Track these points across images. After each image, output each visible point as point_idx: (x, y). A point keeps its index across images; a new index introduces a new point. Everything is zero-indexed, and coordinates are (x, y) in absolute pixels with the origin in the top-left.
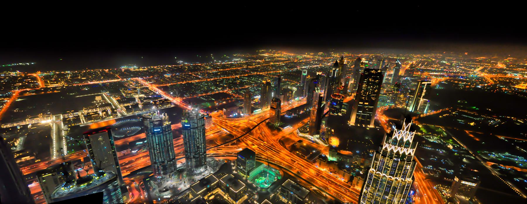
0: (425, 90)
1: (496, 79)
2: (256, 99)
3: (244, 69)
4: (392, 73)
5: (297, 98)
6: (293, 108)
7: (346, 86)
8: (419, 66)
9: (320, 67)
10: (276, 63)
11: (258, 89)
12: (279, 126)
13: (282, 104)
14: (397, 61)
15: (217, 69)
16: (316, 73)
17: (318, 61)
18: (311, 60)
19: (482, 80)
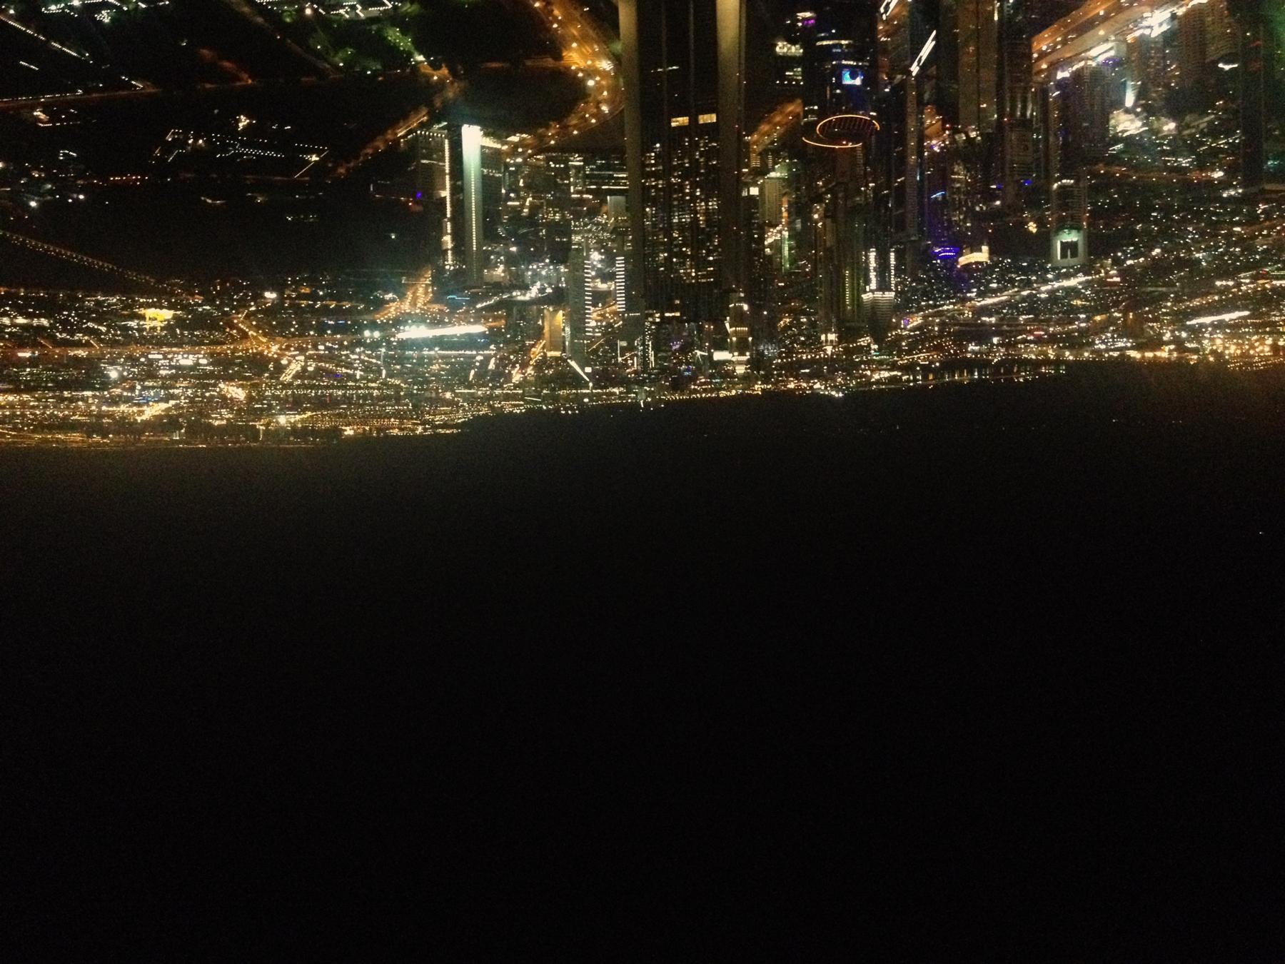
0: (447, 250)
1: (232, 335)
5: (1105, 64)
7: (800, 210)
8: (493, 361)
9: (971, 299)
14: (587, 374)
17: (981, 335)
19: (273, 322)
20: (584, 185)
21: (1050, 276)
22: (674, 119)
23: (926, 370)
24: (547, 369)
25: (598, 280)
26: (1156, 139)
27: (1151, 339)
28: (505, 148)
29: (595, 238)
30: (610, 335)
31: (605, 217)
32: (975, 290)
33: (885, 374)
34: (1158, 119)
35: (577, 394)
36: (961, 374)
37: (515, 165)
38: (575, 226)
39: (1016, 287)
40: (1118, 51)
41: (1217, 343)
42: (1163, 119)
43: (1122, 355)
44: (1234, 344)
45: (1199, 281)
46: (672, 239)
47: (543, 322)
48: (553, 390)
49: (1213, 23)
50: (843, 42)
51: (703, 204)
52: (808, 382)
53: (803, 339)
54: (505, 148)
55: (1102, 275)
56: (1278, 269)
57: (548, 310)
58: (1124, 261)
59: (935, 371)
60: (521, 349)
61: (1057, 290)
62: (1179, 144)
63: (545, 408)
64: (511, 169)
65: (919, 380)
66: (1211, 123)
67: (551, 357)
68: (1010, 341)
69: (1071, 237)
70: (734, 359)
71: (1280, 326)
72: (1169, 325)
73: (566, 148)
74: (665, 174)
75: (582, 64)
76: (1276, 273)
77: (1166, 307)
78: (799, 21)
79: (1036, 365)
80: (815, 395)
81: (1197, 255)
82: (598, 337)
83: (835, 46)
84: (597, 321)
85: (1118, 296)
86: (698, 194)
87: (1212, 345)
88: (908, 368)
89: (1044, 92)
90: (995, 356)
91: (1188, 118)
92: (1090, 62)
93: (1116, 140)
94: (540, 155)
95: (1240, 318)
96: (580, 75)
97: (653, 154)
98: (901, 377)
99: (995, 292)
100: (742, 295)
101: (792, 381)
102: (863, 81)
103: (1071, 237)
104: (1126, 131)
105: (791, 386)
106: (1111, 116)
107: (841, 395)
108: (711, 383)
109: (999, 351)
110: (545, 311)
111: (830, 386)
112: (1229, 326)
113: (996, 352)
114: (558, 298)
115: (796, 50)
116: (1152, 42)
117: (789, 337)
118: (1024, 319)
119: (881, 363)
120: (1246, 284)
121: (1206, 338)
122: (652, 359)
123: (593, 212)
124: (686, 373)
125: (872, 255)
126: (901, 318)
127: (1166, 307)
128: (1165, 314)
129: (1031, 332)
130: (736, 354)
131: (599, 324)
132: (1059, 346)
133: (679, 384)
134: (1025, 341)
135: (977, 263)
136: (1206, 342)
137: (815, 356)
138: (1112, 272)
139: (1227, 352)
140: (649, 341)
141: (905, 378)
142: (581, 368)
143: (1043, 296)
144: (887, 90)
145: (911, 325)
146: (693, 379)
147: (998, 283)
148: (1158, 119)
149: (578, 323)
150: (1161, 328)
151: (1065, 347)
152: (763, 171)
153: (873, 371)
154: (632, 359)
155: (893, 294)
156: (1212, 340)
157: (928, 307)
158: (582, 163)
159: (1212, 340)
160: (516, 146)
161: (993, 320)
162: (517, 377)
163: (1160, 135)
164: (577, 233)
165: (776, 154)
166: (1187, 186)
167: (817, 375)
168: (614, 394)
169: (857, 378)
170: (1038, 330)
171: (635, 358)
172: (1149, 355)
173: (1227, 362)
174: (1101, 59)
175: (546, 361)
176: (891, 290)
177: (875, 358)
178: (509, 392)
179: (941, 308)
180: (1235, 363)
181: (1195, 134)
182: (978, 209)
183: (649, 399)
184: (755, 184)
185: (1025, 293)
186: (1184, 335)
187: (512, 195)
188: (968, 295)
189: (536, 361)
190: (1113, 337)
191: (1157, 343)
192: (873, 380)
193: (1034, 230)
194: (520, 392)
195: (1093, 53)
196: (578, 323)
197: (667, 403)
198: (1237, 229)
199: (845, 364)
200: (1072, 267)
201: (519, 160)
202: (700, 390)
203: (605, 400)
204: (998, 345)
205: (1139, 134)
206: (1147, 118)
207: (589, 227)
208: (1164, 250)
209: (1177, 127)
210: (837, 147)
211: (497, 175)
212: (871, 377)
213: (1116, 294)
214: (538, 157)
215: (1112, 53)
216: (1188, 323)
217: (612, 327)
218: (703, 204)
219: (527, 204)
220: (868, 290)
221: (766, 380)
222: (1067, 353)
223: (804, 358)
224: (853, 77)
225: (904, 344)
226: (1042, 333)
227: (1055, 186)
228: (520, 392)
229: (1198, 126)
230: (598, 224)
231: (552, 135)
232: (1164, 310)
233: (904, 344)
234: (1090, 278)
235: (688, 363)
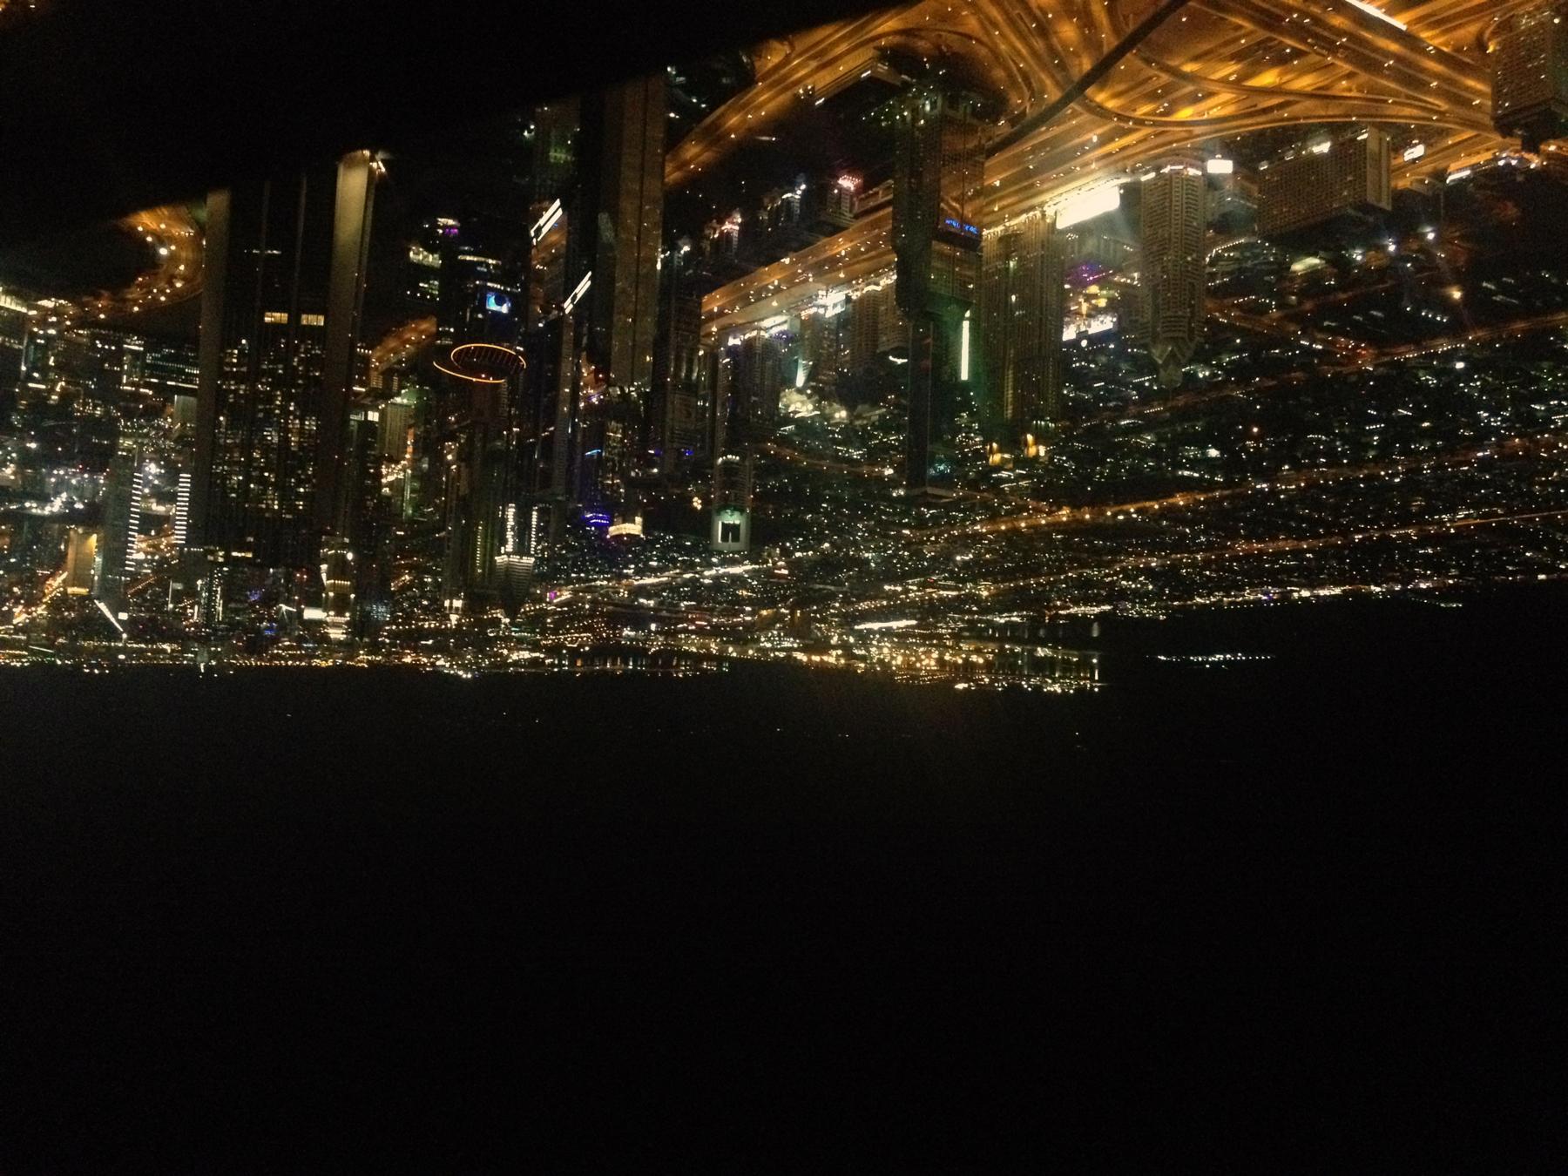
2: (1102, 303)
3: (1209, 547)
4: (138, 550)
5: (778, 337)
7: (429, 447)
9: (627, 577)
10: (955, 593)
11: (1089, 389)
12: (900, 91)
14: (120, 622)
15: (1441, 539)
16: (645, 529)
17: (638, 619)
20: (142, 377)
21: (714, 560)
22: (269, 314)
23: (574, 654)
24: (67, 610)
25: (153, 500)
26: (828, 425)
27: (817, 640)
28: (32, 313)
29: (153, 446)
30: (163, 570)
31: (169, 420)
32: (633, 566)
33: (526, 655)
34: (830, 405)
35: (109, 648)
36: (614, 663)
37: (47, 338)
38: (126, 426)
39: (678, 568)
40: (791, 326)
41: (884, 652)
42: (836, 406)
43: (789, 657)
44: (902, 654)
45: (868, 584)
46: (250, 459)
47: (66, 547)
48: (74, 639)
49: (886, 314)
50: (490, 261)
51: (297, 421)
52: (429, 658)
53: (425, 603)
54: (32, 313)
55: (770, 565)
56: (945, 579)
57: (76, 532)
58: (793, 553)
59: (584, 656)
60: (29, 580)
61: (722, 576)
62: (851, 435)
63: (59, 662)
64: (39, 341)
65: (564, 665)
66: (882, 416)
67: (74, 595)
68: (670, 629)
69: (733, 518)
70: (328, 619)
71: (947, 639)
72: (836, 628)
73: (122, 326)
74: (250, 378)
75: (153, 226)
77: (834, 608)
78: (439, 227)
79: (697, 659)
80: (437, 673)
81: (866, 555)
82: (146, 574)
83: (480, 264)
84: (147, 553)
85: (786, 590)
86: (292, 408)
87: (880, 654)
88: (554, 650)
89: (713, 357)
92: (762, 333)
93: (787, 420)
94: (83, 329)
95: (907, 627)
96: (149, 239)
97: (236, 352)
98: (544, 659)
99: (654, 571)
102: (510, 310)
103: (733, 518)
105: (408, 660)
106: (782, 394)
107: (469, 676)
108: (300, 648)
109: (657, 639)
110: (72, 533)
111: (457, 664)
112: (898, 635)
113: (653, 641)
114: (91, 518)
115: (433, 260)
116: (825, 323)
117: (408, 598)
118: (686, 606)
119: (520, 641)
120: (914, 591)
121: (874, 646)
122: (220, 609)
123: (154, 412)
124: (268, 633)
125: (511, 512)
126: (547, 590)
127: (834, 608)
128: (833, 615)
129: (692, 621)
130: (332, 613)
131: (149, 557)
132: (722, 640)
133: (257, 645)
134: (685, 630)
135: (628, 535)
136: (873, 650)
137: (440, 626)
138: (780, 563)
139: (894, 662)
140: (217, 586)
141: (548, 661)
142: (112, 613)
143: (707, 581)
144: (541, 325)
145: (558, 600)
146: (275, 641)
147: (658, 561)
148: (830, 405)
149: (115, 553)
150: (829, 631)
151: (731, 643)
152: (386, 394)
153: (510, 650)
154: (192, 608)
155: (533, 560)
156: (880, 648)
157: (579, 580)
158: (142, 349)
159: (880, 648)
160: (46, 312)
161: (652, 603)
162: (20, 617)
163: (832, 422)
164: (126, 436)
165: (404, 375)
166: (857, 480)
167: (441, 648)
168: (164, 651)
169: (489, 657)
170: (700, 620)
171: (196, 607)
172: (816, 658)
173: (894, 674)
174: (774, 331)
175: (67, 600)
176: (532, 556)
178: (6, 636)
180: (902, 675)
181: (867, 425)
182: (633, 474)
183: (214, 663)
184: (375, 408)
185: (687, 576)
186: (852, 640)
187: (36, 375)
188: (625, 571)
189: (51, 599)
190: (779, 635)
191: (823, 647)
192: (510, 661)
193: (699, 507)
194: (23, 638)
195: (766, 323)
196: (115, 553)
197: (238, 669)
198: (907, 532)
199: (475, 637)
200: (739, 552)
201: (52, 332)
202: (284, 654)
203: (149, 658)
204: (656, 632)
206: (820, 402)
207: (145, 430)
208: (833, 544)
209: (849, 416)
210: (474, 380)
211: (16, 347)
212: (508, 657)
213: (783, 588)
214: (81, 332)
215: (785, 327)
216: (856, 627)
217: (169, 564)
218: (297, 421)
219: (58, 389)
220: (503, 551)
221: (374, 648)
222: (731, 649)
223: (426, 626)
224: (499, 302)
225: (549, 621)
227: (720, 460)
228: (23, 638)
230: (159, 428)
231: (101, 308)
232: (832, 611)
233: (549, 621)
234: (757, 567)
235: (271, 620)
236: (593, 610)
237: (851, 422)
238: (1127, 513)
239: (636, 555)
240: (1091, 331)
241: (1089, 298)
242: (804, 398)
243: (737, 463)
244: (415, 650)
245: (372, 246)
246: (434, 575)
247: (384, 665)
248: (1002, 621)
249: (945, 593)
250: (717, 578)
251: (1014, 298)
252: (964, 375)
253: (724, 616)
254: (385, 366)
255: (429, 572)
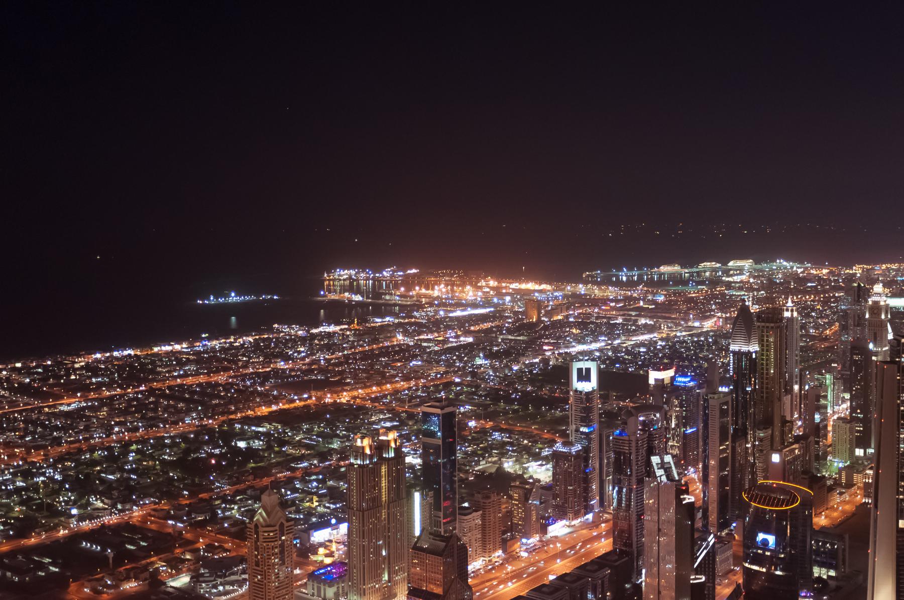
2: (322, 551)
3: (244, 377)
6: (544, 585)
7: (818, 431)
9: (662, 339)
10: (422, 337)
11: (330, 489)
13: (476, 565)
18: (613, 309)
21: (597, 354)
32: (658, 347)
42: (511, 471)
45: (485, 342)
56: (429, 347)
61: (591, 342)
70: (885, 298)
76: (431, 345)
77: (509, 323)
90: (642, 290)
91: (493, 470)
92: (567, 523)
95: (455, 311)
99: (642, 344)
100: (874, 358)
101: (824, 275)
104: (539, 465)
106: (551, 478)
117: (827, 316)
119: (741, 289)
120: (452, 337)
128: (509, 317)
143: (603, 338)
150: (513, 307)
157: (699, 335)
165: (837, 483)
167: (802, 280)
176: (732, 352)
177: (746, 294)
179: (688, 333)
182: (658, 415)
185: (617, 342)
198: (457, 380)
205: (528, 462)
206: (524, 473)
209: (502, 463)
210: (781, 482)
216: (492, 309)
221: (851, 278)
224: (765, 542)
226: (603, 307)
229: (486, 463)
232: (510, 320)
234: (566, 350)
236: (687, 313)
237: (500, 460)
238: (300, 400)
239: (656, 355)
240: (329, 530)
241: (330, 555)
242: (535, 476)
243: (582, 426)
244: (819, 279)
245: (866, 580)
246: (808, 335)
247: (843, 266)
248: (387, 319)
249: (430, 336)
250: (596, 340)
251: (384, 553)
252: (417, 496)
253: (589, 314)
254: (853, 490)
255: (813, 338)
